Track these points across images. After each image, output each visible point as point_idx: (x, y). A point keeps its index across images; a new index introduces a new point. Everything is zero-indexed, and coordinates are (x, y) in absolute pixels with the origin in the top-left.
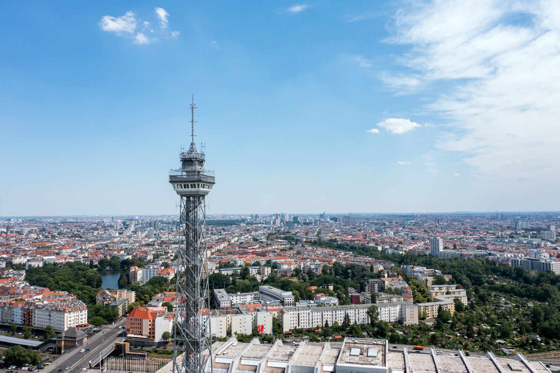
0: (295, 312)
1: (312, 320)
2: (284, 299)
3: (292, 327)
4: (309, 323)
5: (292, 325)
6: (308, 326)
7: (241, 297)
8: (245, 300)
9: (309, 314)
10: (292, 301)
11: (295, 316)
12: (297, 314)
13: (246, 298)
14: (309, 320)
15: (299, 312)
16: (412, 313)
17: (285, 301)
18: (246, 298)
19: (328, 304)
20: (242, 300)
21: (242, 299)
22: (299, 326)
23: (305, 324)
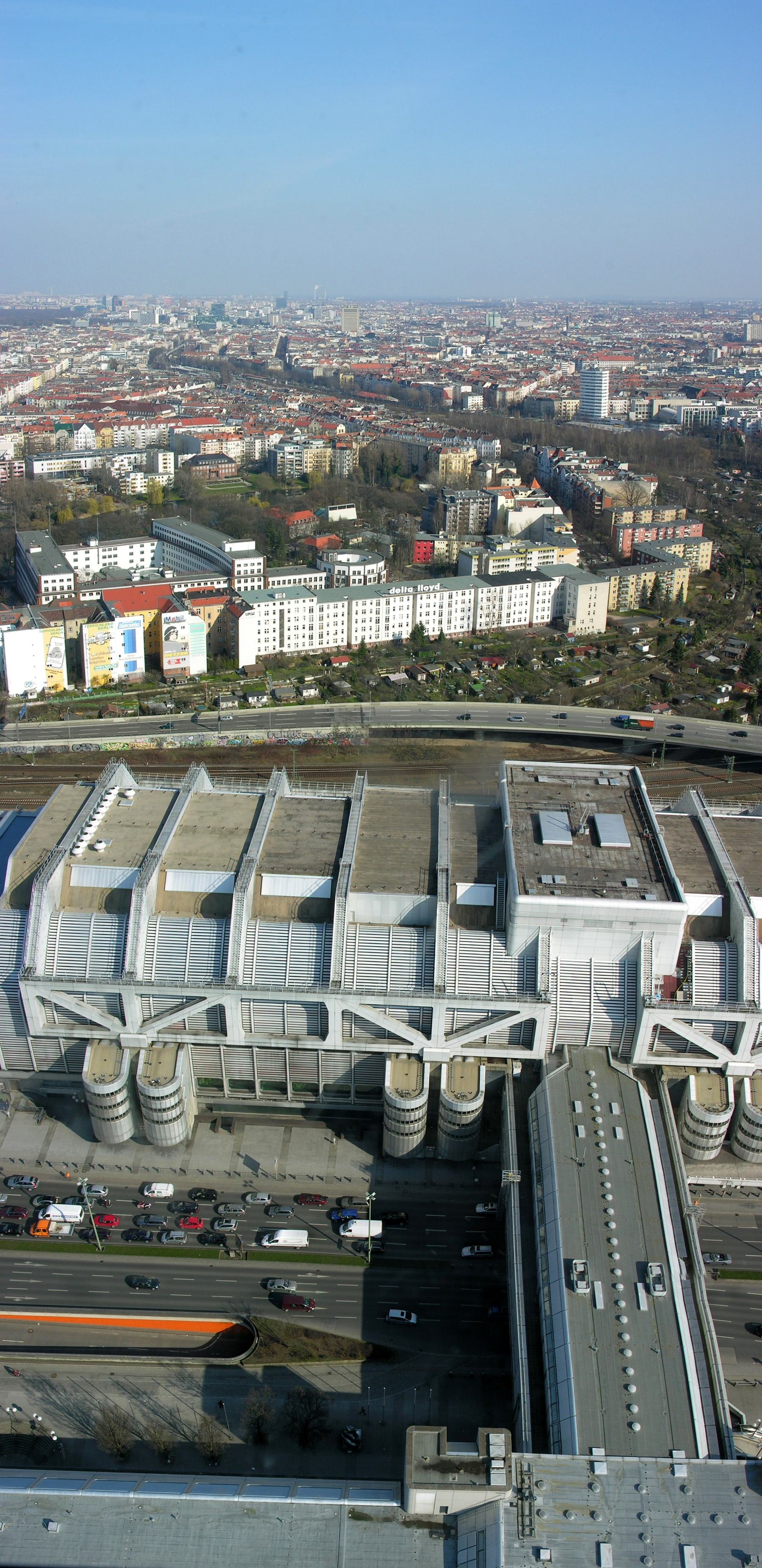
0: (271, 608)
1: (321, 627)
2: (232, 564)
3: (263, 649)
4: (311, 637)
5: (263, 645)
6: (307, 644)
7: (102, 554)
8: (113, 560)
9: (311, 610)
10: (256, 568)
11: (271, 617)
12: (278, 613)
13: (115, 556)
14: (311, 628)
15: (282, 607)
16: (593, 601)
17: (237, 569)
18: (115, 556)
19: (359, 573)
20: (102, 561)
21: (104, 557)
22: (282, 644)
23: (300, 641)
